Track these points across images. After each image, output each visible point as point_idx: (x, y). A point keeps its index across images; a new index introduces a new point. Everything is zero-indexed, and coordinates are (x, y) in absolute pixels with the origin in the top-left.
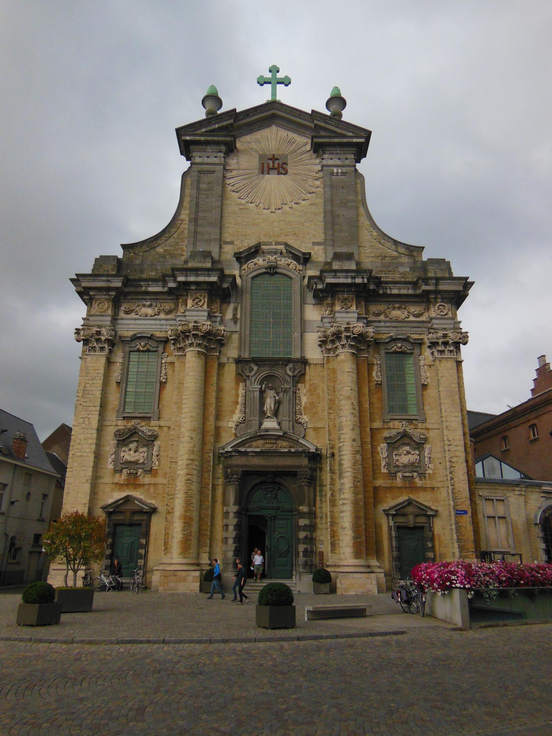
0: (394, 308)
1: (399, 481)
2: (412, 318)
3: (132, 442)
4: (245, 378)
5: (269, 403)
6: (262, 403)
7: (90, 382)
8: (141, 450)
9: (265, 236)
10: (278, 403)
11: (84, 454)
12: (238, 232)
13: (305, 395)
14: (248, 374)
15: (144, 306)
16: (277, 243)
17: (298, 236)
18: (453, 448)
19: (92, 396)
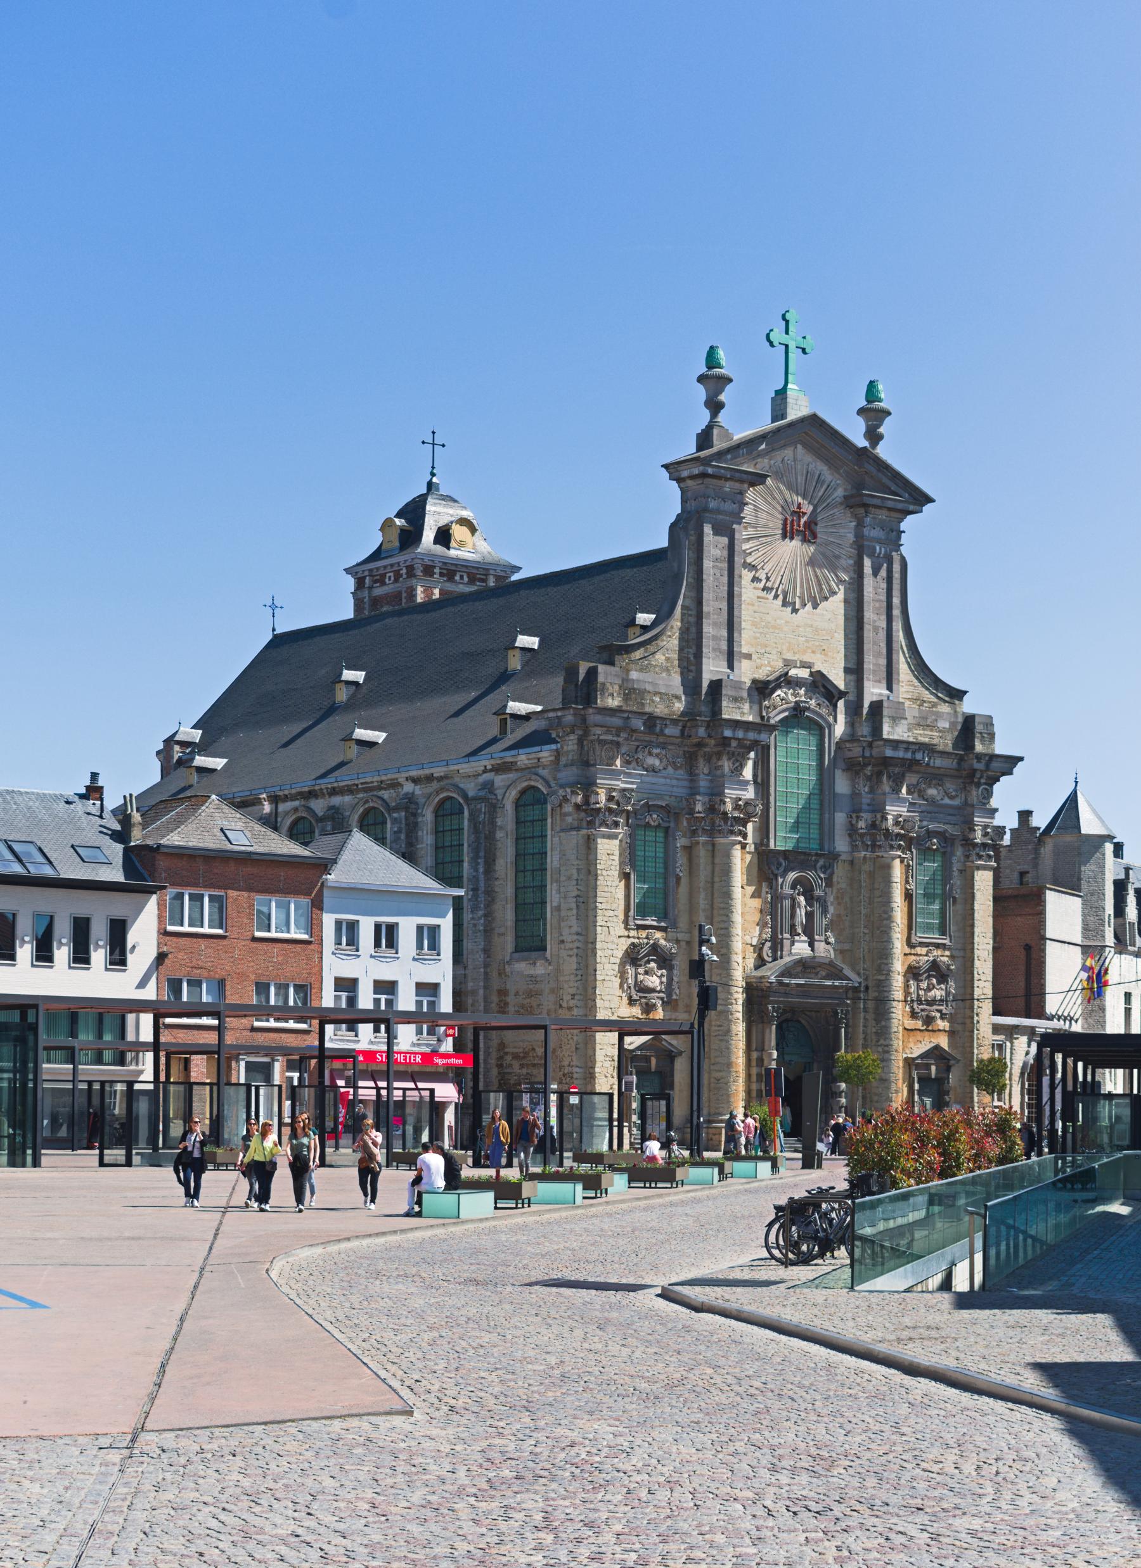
0: (930, 787)
1: (919, 1024)
2: (947, 801)
3: (648, 962)
4: (771, 876)
5: (801, 914)
6: (793, 916)
7: (604, 873)
8: (660, 972)
9: (789, 650)
10: (809, 916)
11: (607, 978)
12: (756, 638)
13: (832, 904)
14: (776, 872)
15: (650, 754)
16: (805, 665)
17: (826, 655)
18: (981, 984)
19: (608, 895)
